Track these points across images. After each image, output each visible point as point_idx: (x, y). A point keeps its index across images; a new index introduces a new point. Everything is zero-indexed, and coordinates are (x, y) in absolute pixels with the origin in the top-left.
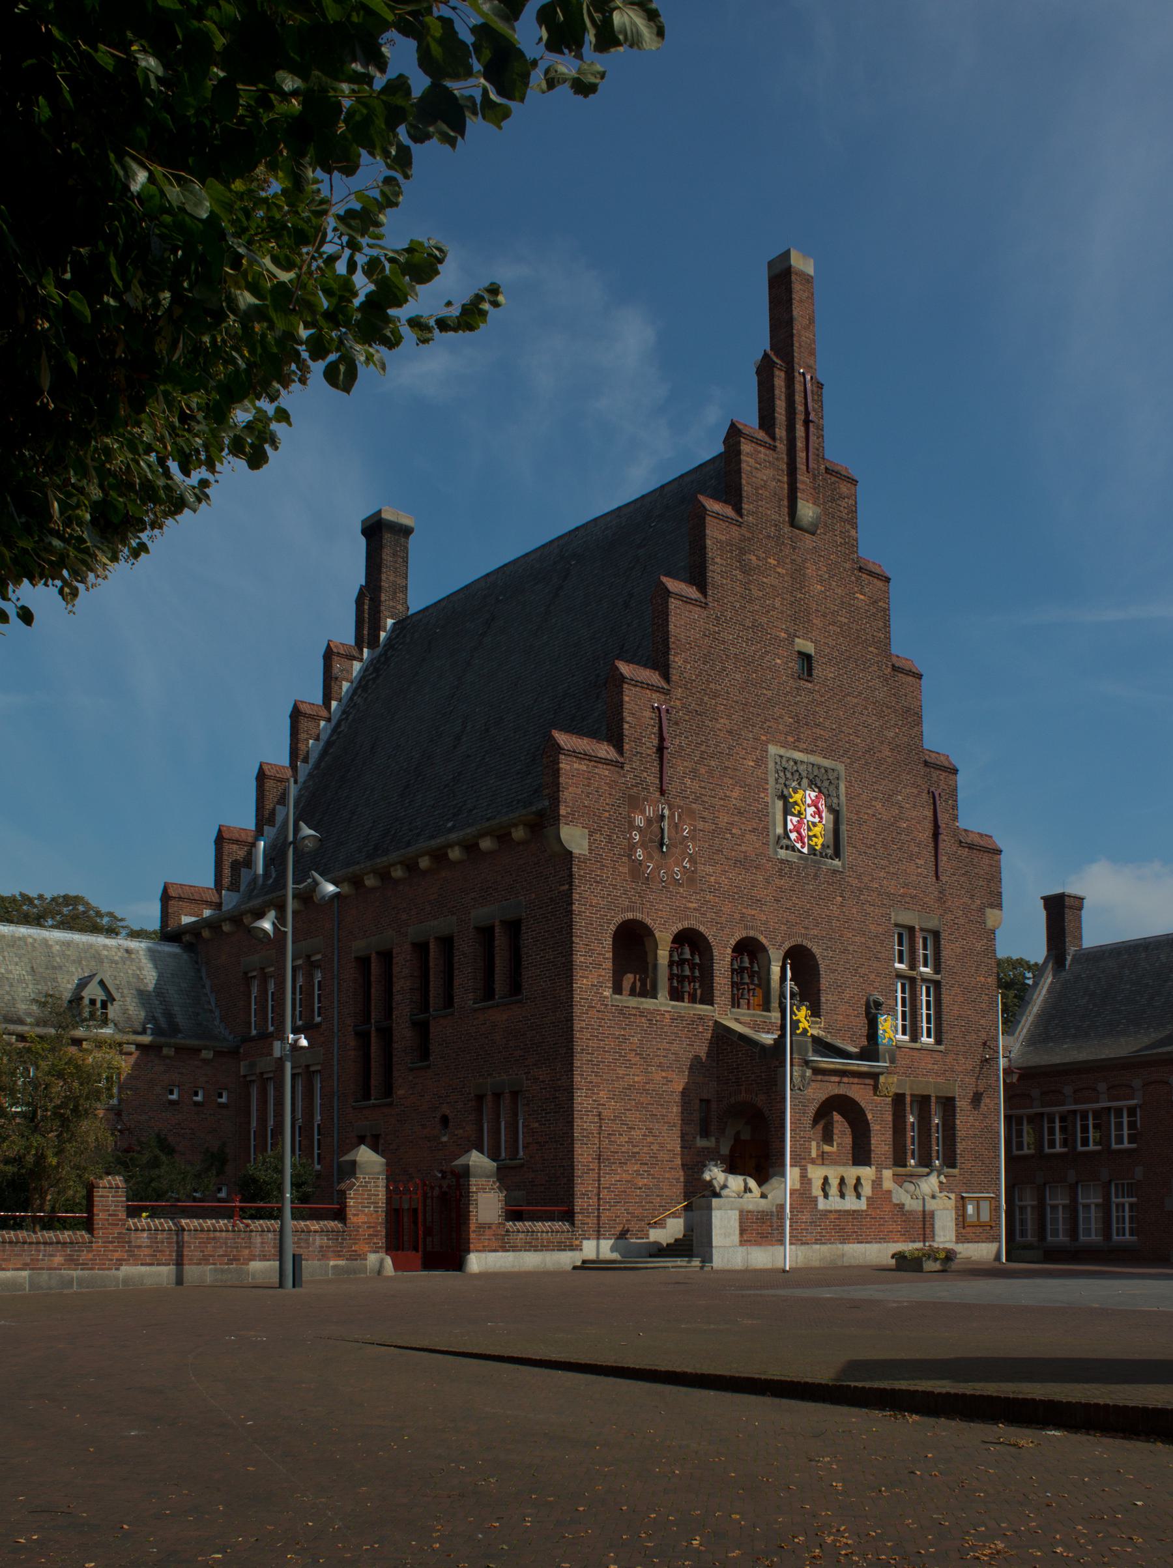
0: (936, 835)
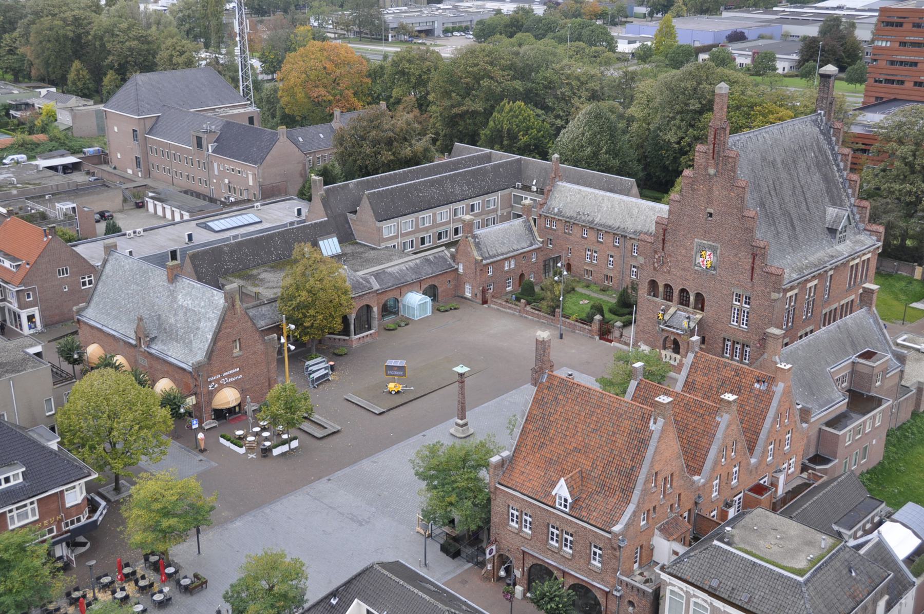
0: (753, 268)
